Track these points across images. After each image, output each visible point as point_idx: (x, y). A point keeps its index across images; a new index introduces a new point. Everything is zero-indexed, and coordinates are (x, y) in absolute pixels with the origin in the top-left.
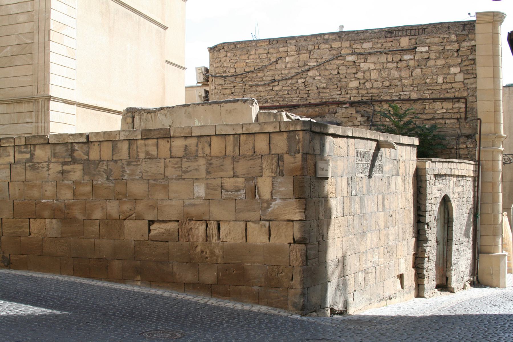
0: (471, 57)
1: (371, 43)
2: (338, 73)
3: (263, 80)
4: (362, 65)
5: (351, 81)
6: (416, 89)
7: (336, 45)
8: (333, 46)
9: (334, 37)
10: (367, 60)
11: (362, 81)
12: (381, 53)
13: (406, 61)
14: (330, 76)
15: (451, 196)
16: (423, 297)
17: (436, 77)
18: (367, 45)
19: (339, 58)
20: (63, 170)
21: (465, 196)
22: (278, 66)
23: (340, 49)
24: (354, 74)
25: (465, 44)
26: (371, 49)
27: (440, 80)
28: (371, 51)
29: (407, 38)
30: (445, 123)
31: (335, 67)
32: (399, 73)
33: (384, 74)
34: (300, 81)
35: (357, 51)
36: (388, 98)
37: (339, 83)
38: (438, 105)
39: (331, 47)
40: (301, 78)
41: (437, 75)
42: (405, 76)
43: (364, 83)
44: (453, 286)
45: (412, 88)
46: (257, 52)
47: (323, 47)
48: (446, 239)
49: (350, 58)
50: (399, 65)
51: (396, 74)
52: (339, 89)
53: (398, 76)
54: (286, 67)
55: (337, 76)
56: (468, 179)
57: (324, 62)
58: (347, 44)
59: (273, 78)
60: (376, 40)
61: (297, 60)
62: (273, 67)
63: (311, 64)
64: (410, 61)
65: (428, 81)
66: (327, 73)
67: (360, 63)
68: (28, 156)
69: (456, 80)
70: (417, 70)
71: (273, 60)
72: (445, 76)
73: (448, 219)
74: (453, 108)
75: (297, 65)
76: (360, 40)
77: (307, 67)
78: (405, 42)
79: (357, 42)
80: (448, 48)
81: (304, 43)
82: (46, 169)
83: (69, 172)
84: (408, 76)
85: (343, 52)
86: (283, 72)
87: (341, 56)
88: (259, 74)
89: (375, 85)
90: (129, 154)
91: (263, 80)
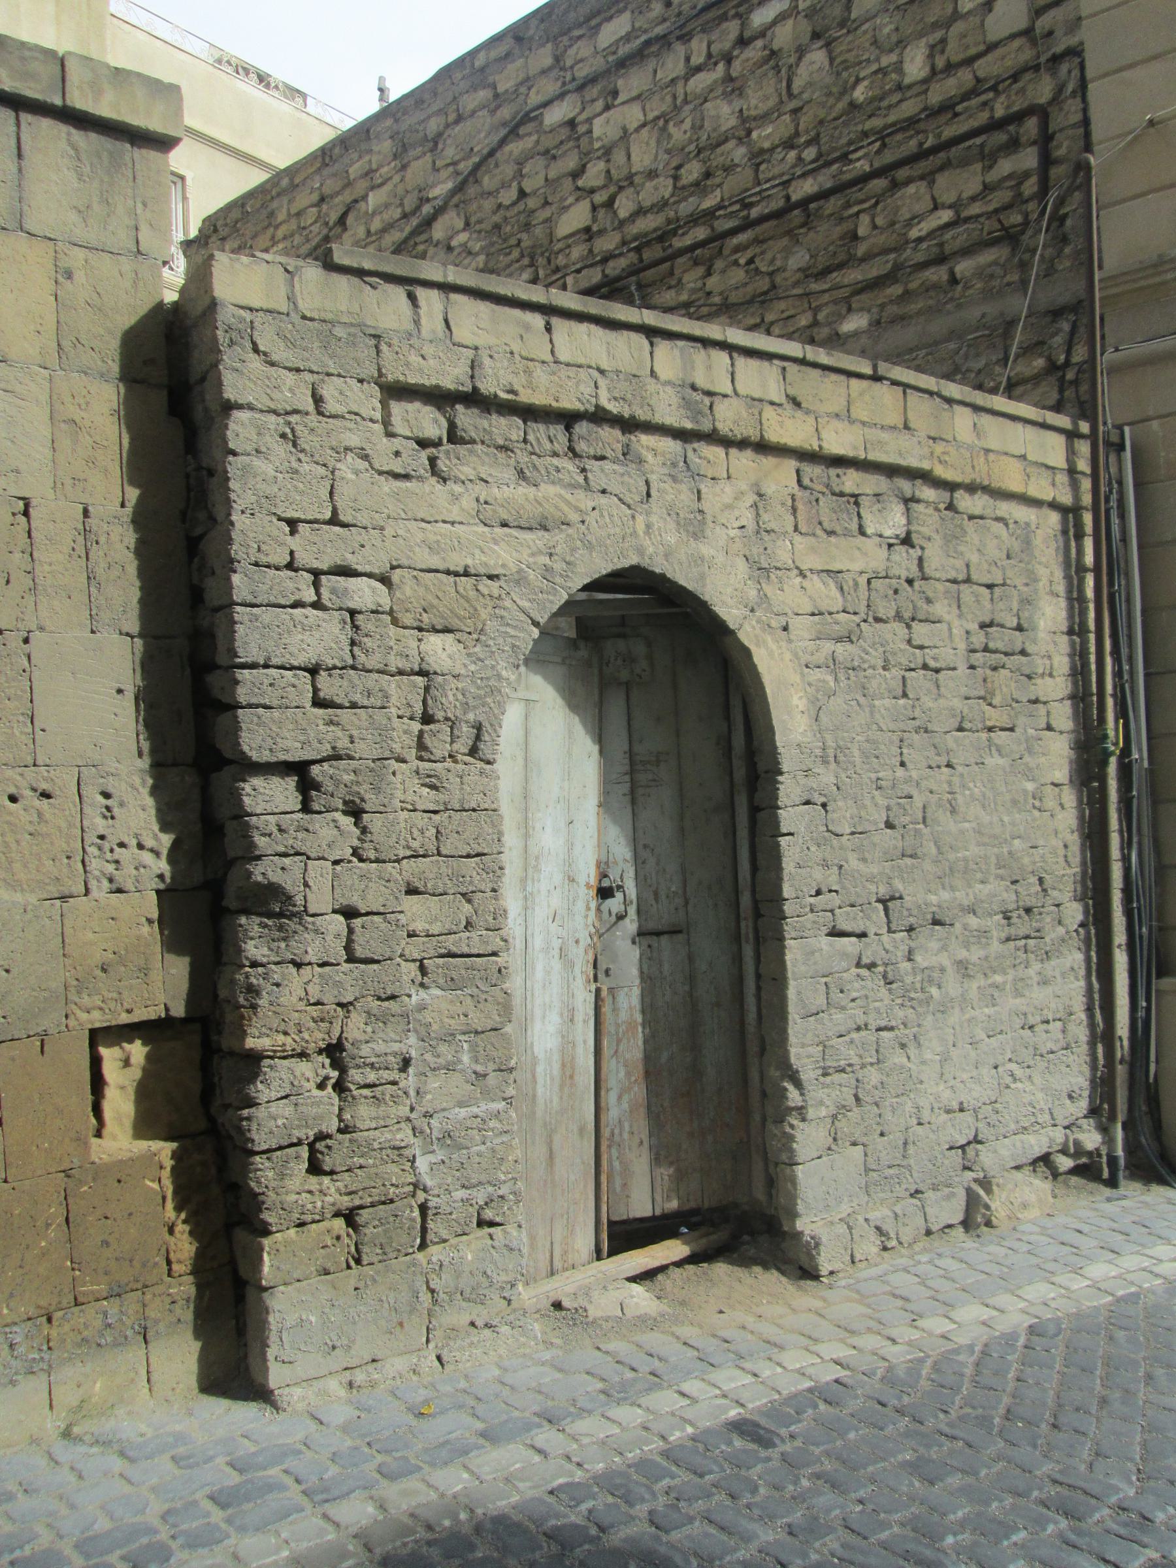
1: (627, 15)
5: (565, 209)
6: (810, 153)
9: (502, 49)
10: (615, 93)
11: (600, 198)
12: (664, 41)
13: (762, 34)
14: (497, 218)
15: (726, 592)
16: (260, 1393)
17: (893, 58)
19: (521, 131)
21: (940, 609)
23: (523, 90)
26: (627, 38)
27: (915, 66)
30: (954, 280)
31: (509, 170)
32: (738, 104)
33: (678, 134)
35: (582, 72)
36: (701, 233)
37: (524, 236)
38: (914, 197)
39: (496, 96)
41: (901, 44)
42: (763, 108)
43: (610, 203)
44: (807, 1224)
45: (792, 154)
47: (471, 107)
48: (746, 899)
50: (737, 68)
51: (723, 113)
52: (526, 261)
53: (733, 122)
54: (369, 232)
55: (516, 210)
56: (967, 502)
57: (477, 167)
61: (400, 190)
64: (778, 29)
65: (859, 94)
66: (488, 204)
67: (589, 121)
69: (992, 37)
70: (809, 57)
72: (938, 35)
73: (751, 754)
74: (987, 188)
76: (588, 20)
77: (427, 209)
79: (576, 33)
84: (771, 103)
89: (649, 193)
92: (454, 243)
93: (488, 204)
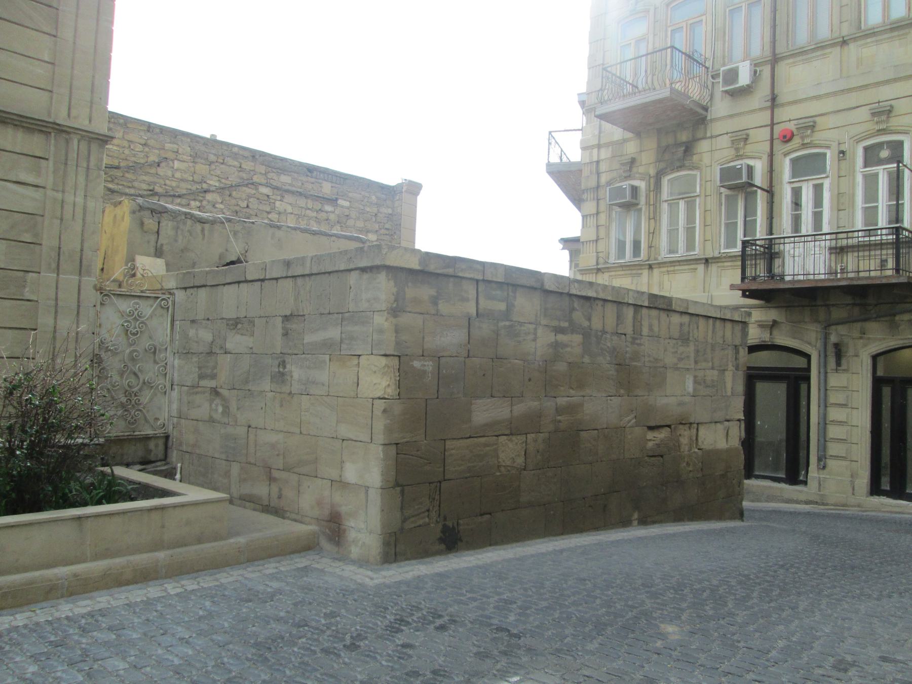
0: (387, 226)
2: (248, 206)
3: (133, 187)
4: (278, 204)
7: (248, 165)
8: (244, 166)
9: (246, 154)
12: (300, 194)
13: (327, 212)
14: (237, 208)
18: (285, 179)
20: (556, 342)
22: (161, 171)
24: (268, 213)
25: (384, 210)
26: (290, 185)
28: (290, 188)
29: (329, 185)
31: (244, 196)
34: (193, 203)
40: (195, 200)
46: (127, 137)
49: (264, 190)
55: (245, 210)
57: (232, 186)
58: (262, 169)
59: (151, 188)
60: (296, 175)
62: (153, 171)
63: (211, 182)
66: (233, 202)
68: (502, 306)
71: (153, 158)
75: (191, 178)
77: (205, 186)
78: (327, 189)
80: (368, 209)
81: (203, 148)
82: (531, 337)
83: (566, 346)
85: (256, 179)
86: (168, 182)
87: (252, 184)
88: (127, 175)
90: (634, 326)
91: (133, 187)
92: (217, 206)
93: (233, 202)
